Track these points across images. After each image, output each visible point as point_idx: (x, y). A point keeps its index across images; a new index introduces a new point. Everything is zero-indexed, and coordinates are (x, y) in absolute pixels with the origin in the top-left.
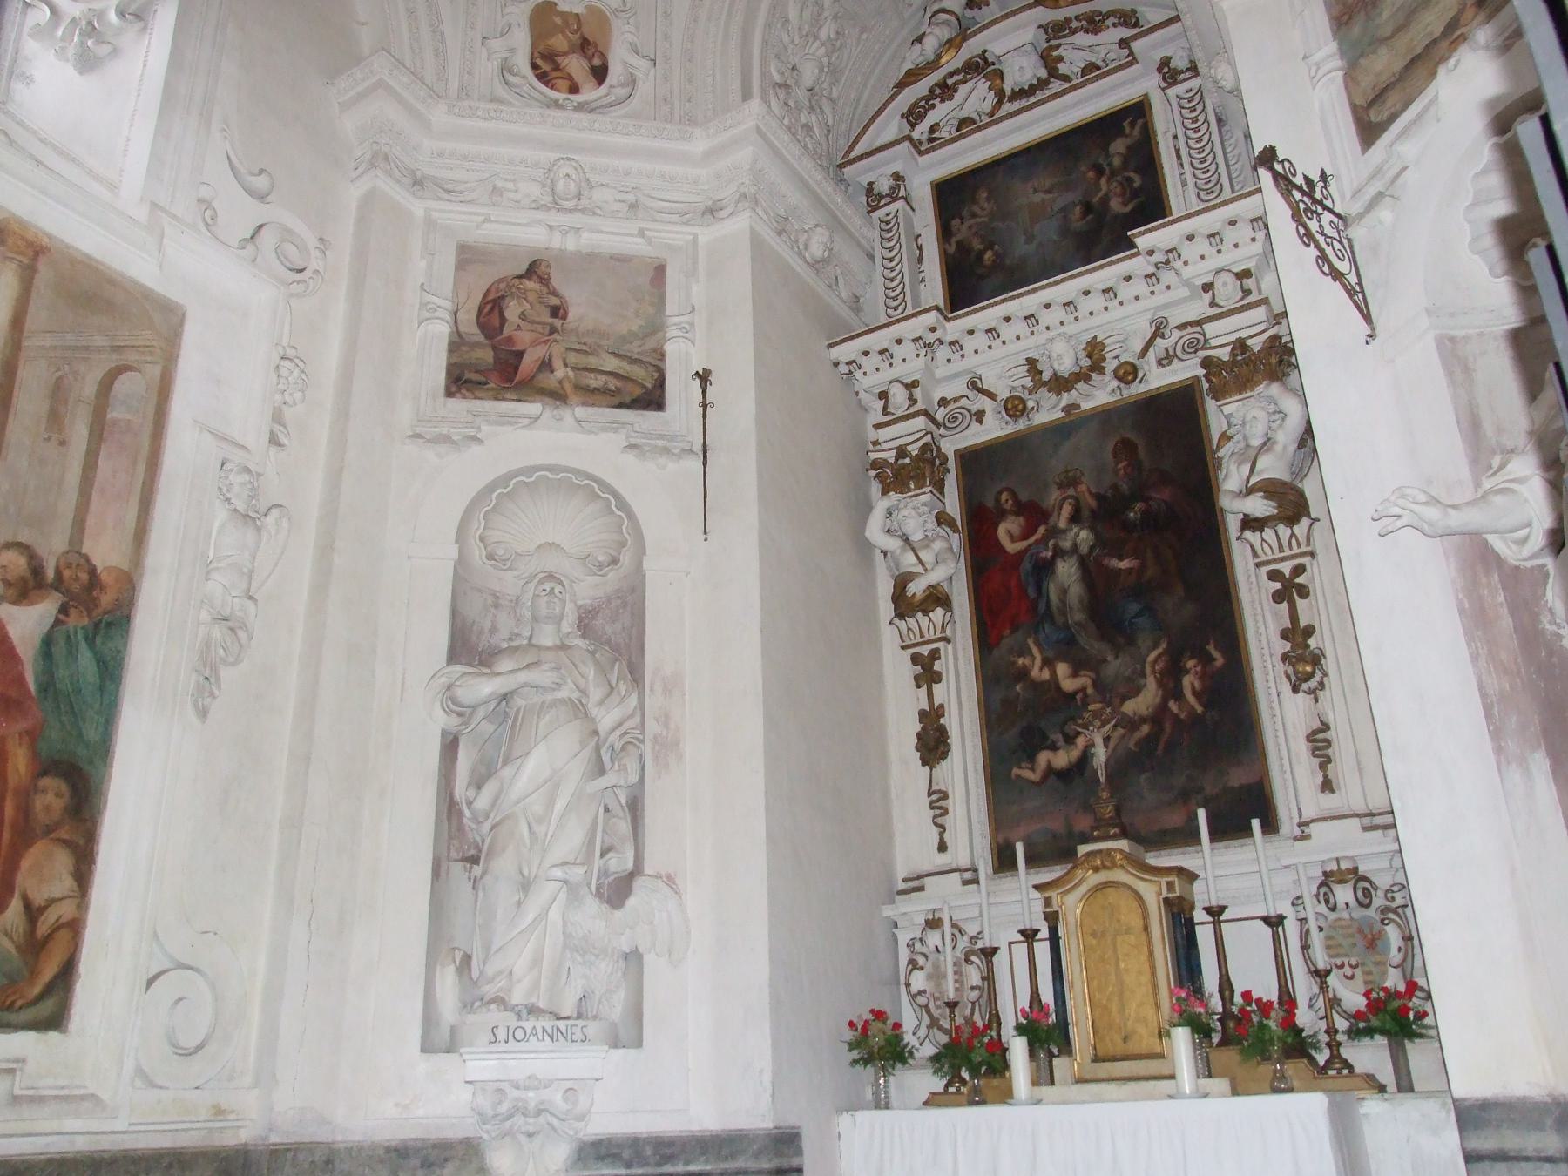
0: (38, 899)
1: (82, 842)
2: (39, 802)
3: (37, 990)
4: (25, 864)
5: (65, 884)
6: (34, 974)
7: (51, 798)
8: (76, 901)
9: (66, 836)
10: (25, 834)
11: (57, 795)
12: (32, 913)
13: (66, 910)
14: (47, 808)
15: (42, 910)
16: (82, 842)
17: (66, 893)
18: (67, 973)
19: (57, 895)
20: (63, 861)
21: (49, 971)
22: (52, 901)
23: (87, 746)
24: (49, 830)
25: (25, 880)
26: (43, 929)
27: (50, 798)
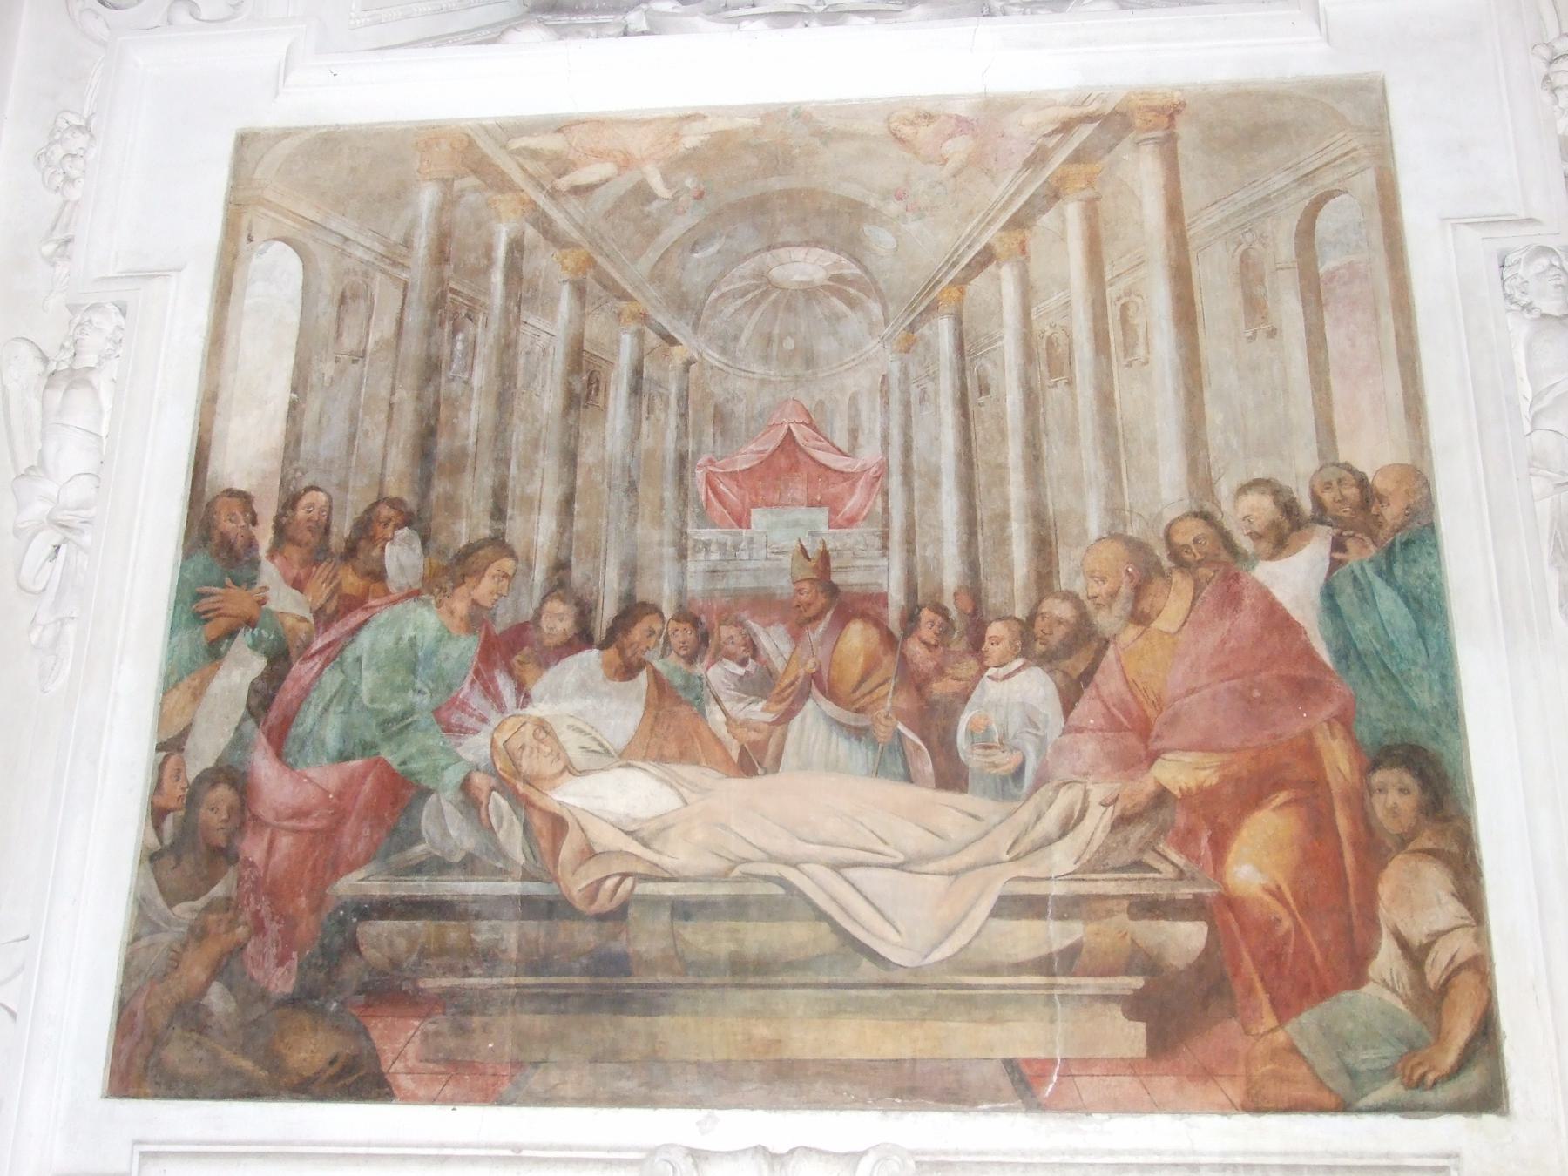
0: (1417, 934)
1: (1455, 849)
2: (1380, 806)
3: (1451, 1058)
4: (1385, 890)
5: (1448, 911)
6: (1439, 1036)
7: (1395, 797)
8: (1472, 931)
9: (1430, 845)
10: (1375, 850)
11: (1403, 791)
12: (1415, 955)
13: (1460, 945)
14: (1394, 811)
15: (1426, 948)
16: (1455, 849)
17: (1460, 922)
18: (1487, 1031)
19: (1440, 925)
20: (1435, 879)
21: (1461, 1030)
22: (1436, 937)
23: (1423, 715)
24: (1403, 842)
25: (1389, 913)
26: (1434, 975)
27: (1393, 797)
